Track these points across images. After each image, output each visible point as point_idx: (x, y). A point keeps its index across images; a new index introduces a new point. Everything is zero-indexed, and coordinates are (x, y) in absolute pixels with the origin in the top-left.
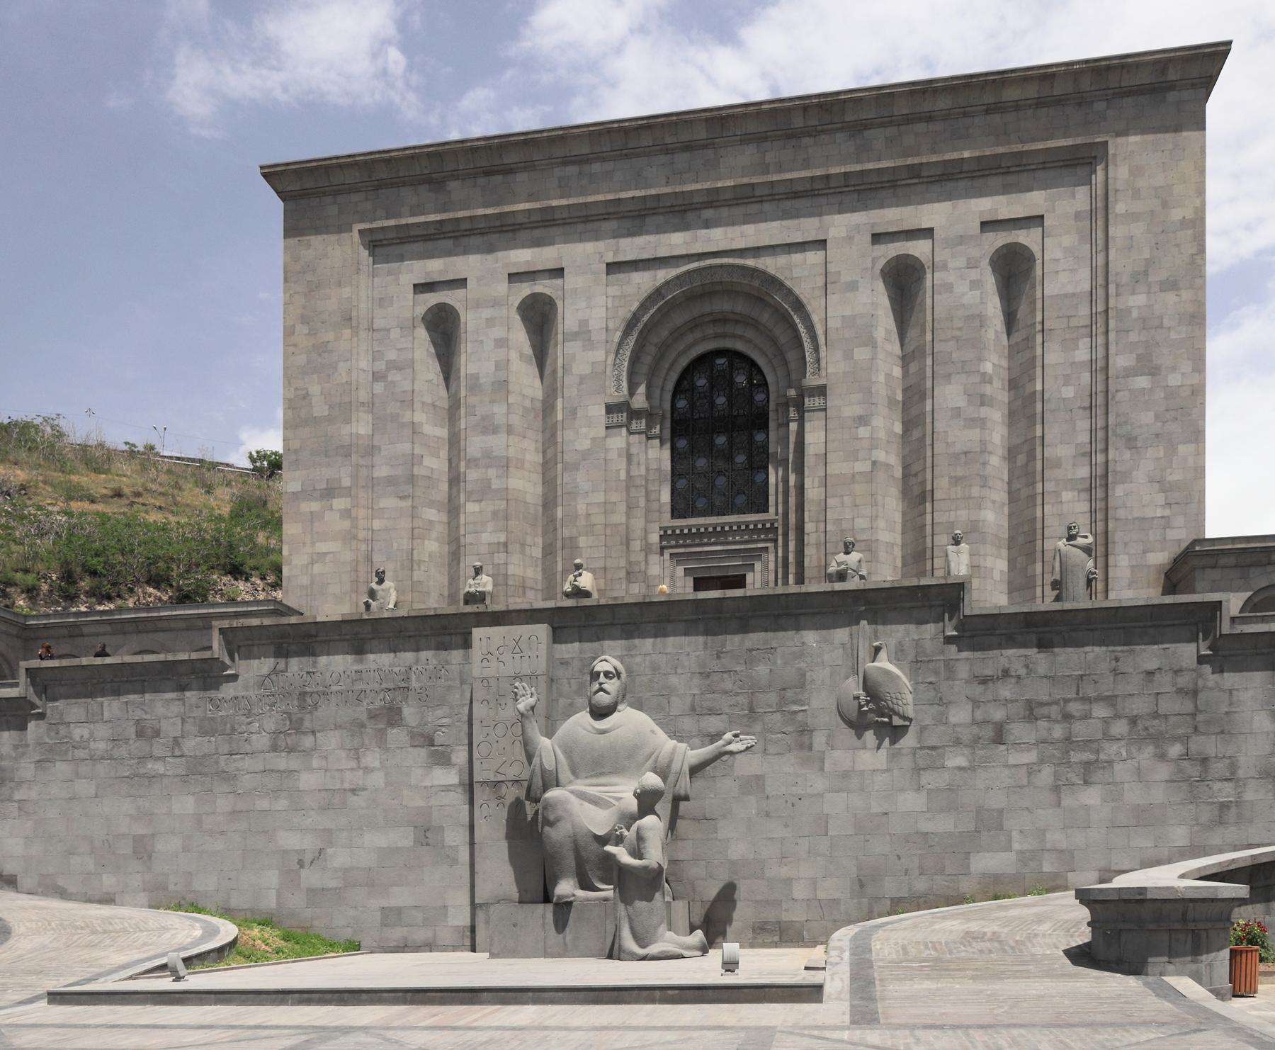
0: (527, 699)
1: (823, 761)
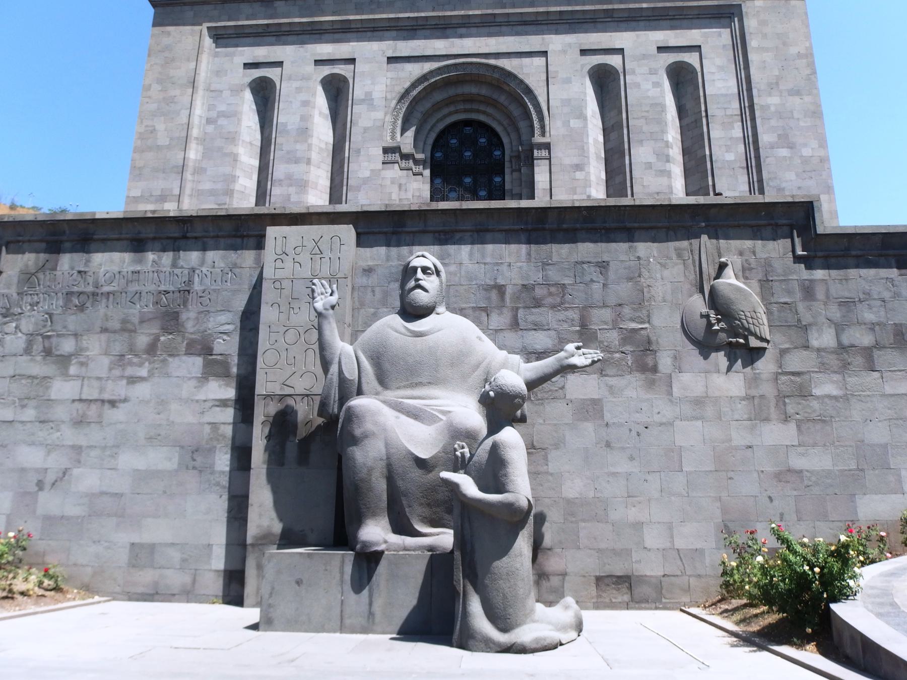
0: (326, 297)
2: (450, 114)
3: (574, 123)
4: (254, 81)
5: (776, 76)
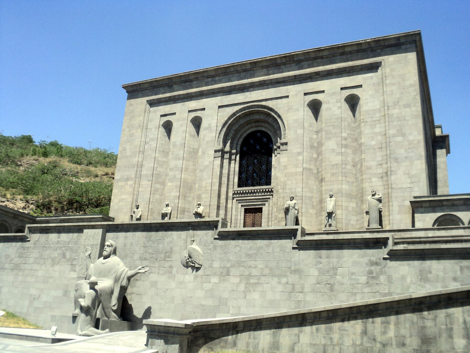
1: (174, 277)
2: (249, 129)
3: (300, 131)
4: (164, 122)
5: (398, 98)
